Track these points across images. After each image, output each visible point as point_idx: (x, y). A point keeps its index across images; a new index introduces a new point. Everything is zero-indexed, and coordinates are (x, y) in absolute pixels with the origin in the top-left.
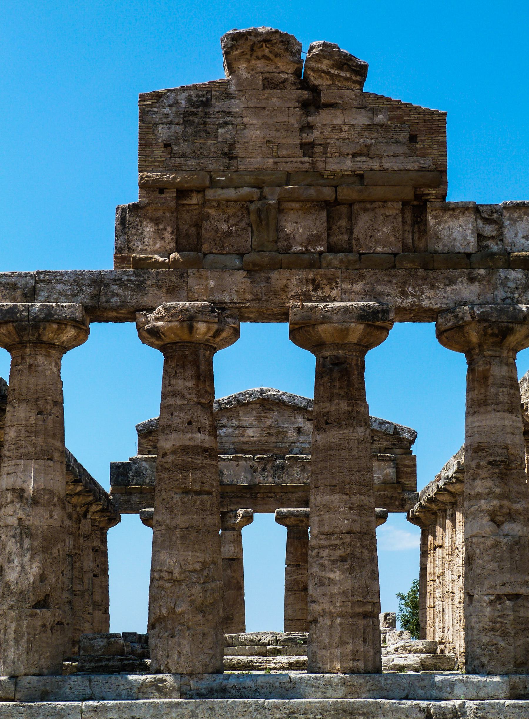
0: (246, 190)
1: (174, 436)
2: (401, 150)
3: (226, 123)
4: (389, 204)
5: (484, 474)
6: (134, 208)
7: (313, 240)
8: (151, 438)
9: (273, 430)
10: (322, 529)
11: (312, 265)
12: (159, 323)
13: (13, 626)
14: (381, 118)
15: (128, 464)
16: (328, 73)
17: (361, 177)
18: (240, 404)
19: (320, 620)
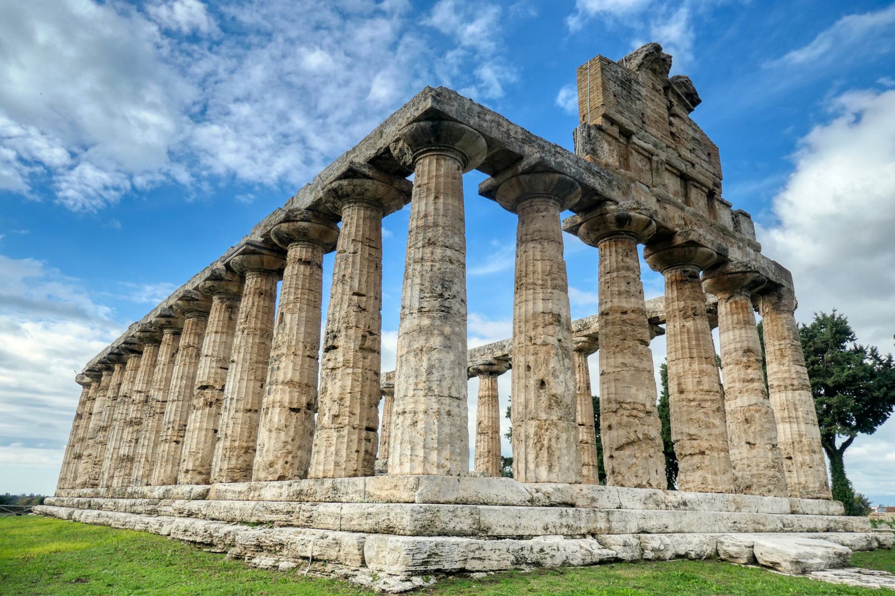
0: (649, 146)
1: (633, 299)
2: (707, 159)
3: (639, 99)
4: (704, 188)
5: (755, 366)
6: (599, 128)
7: (676, 194)
10: (701, 387)
11: (682, 209)
12: (632, 213)
13: (564, 436)
14: (697, 136)
16: (678, 96)
17: (693, 165)
19: (707, 452)
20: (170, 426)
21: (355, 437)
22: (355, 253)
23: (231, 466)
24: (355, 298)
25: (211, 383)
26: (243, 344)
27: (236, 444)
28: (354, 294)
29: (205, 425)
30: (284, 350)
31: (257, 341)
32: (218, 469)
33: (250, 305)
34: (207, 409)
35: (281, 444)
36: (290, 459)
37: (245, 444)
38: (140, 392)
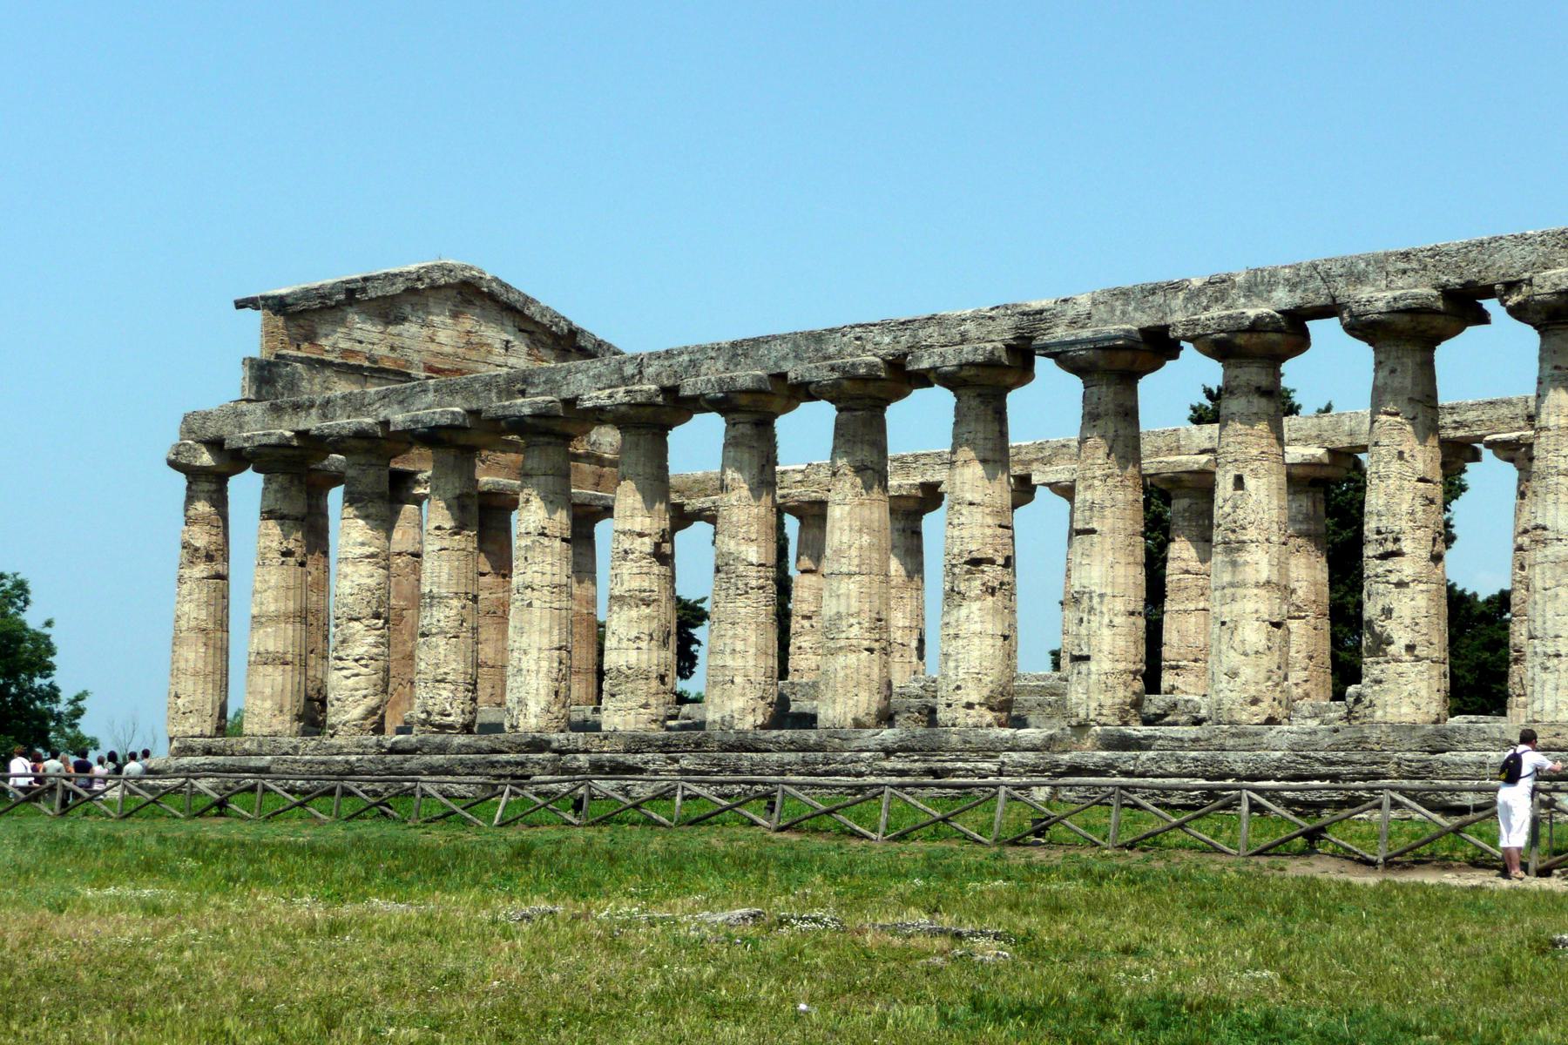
8: (302, 322)
9: (475, 339)
15: (275, 365)
18: (434, 288)
20: (852, 620)
21: (1435, 673)
22: (1414, 418)
23: (1117, 700)
24: (1421, 485)
25: (989, 553)
26: (1108, 503)
27: (1121, 666)
28: (1420, 480)
29: (989, 628)
30: (1251, 533)
31: (1131, 497)
32: (1094, 705)
33: (1111, 433)
34: (990, 598)
35: (1262, 675)
36: (1277, 695)
37: (1132, 667)
38: (641, 535)
